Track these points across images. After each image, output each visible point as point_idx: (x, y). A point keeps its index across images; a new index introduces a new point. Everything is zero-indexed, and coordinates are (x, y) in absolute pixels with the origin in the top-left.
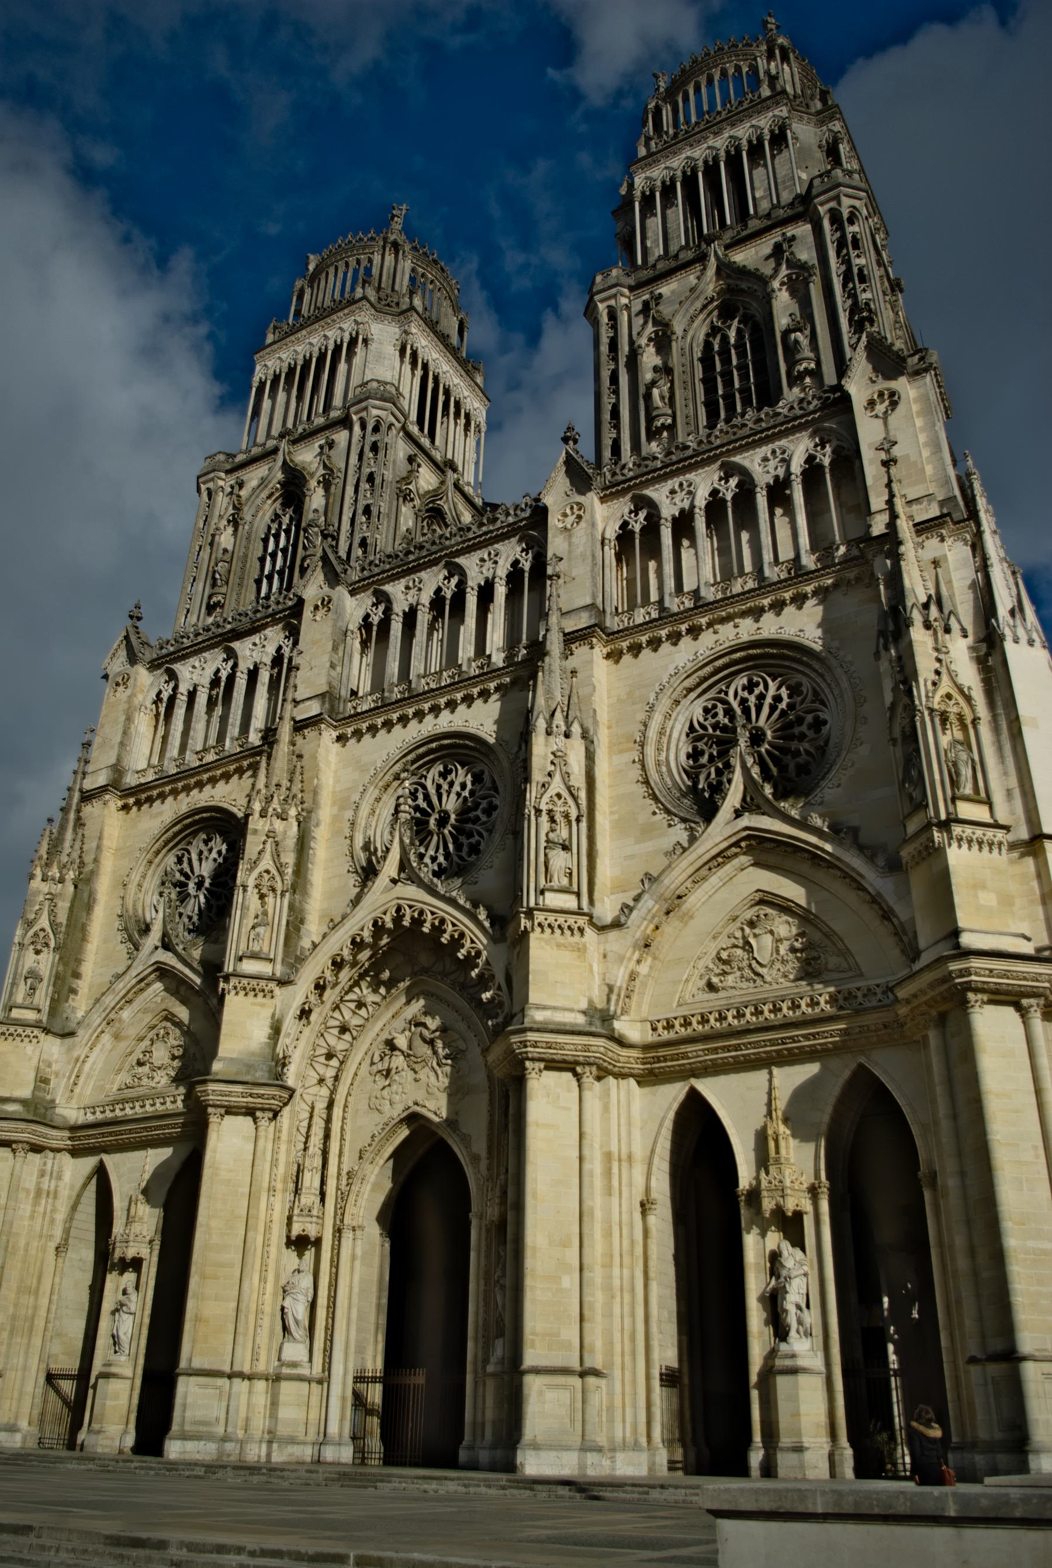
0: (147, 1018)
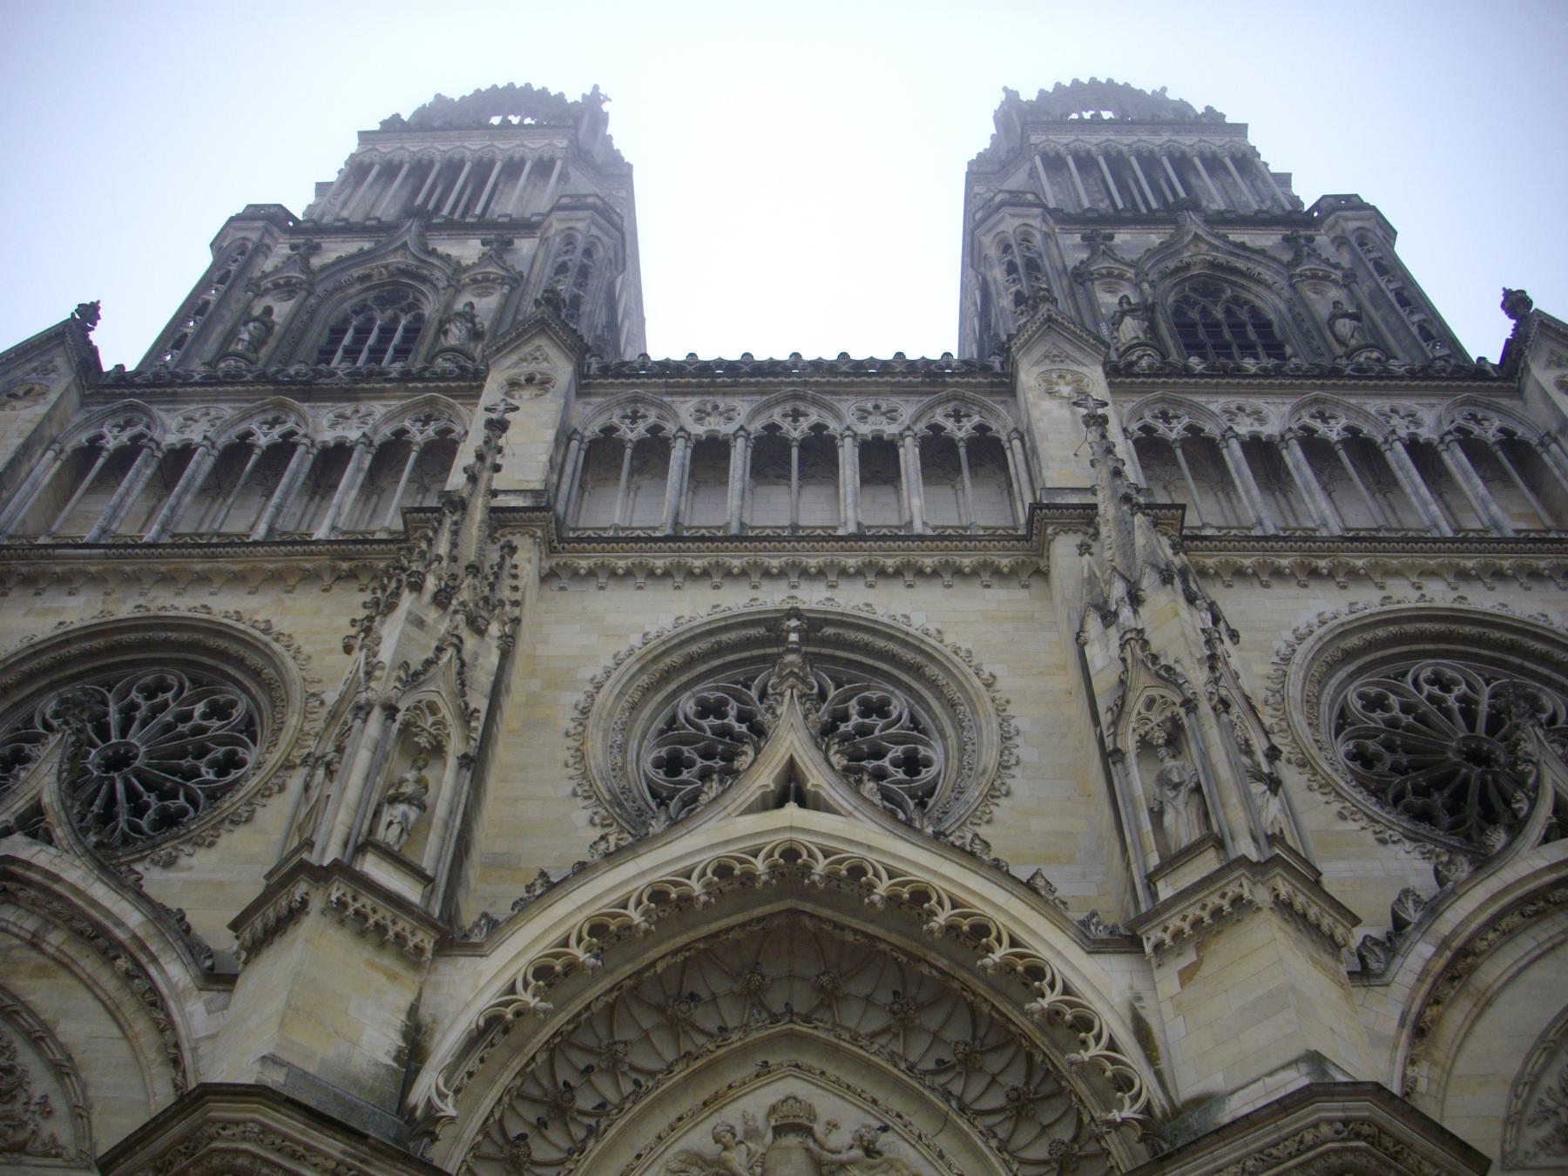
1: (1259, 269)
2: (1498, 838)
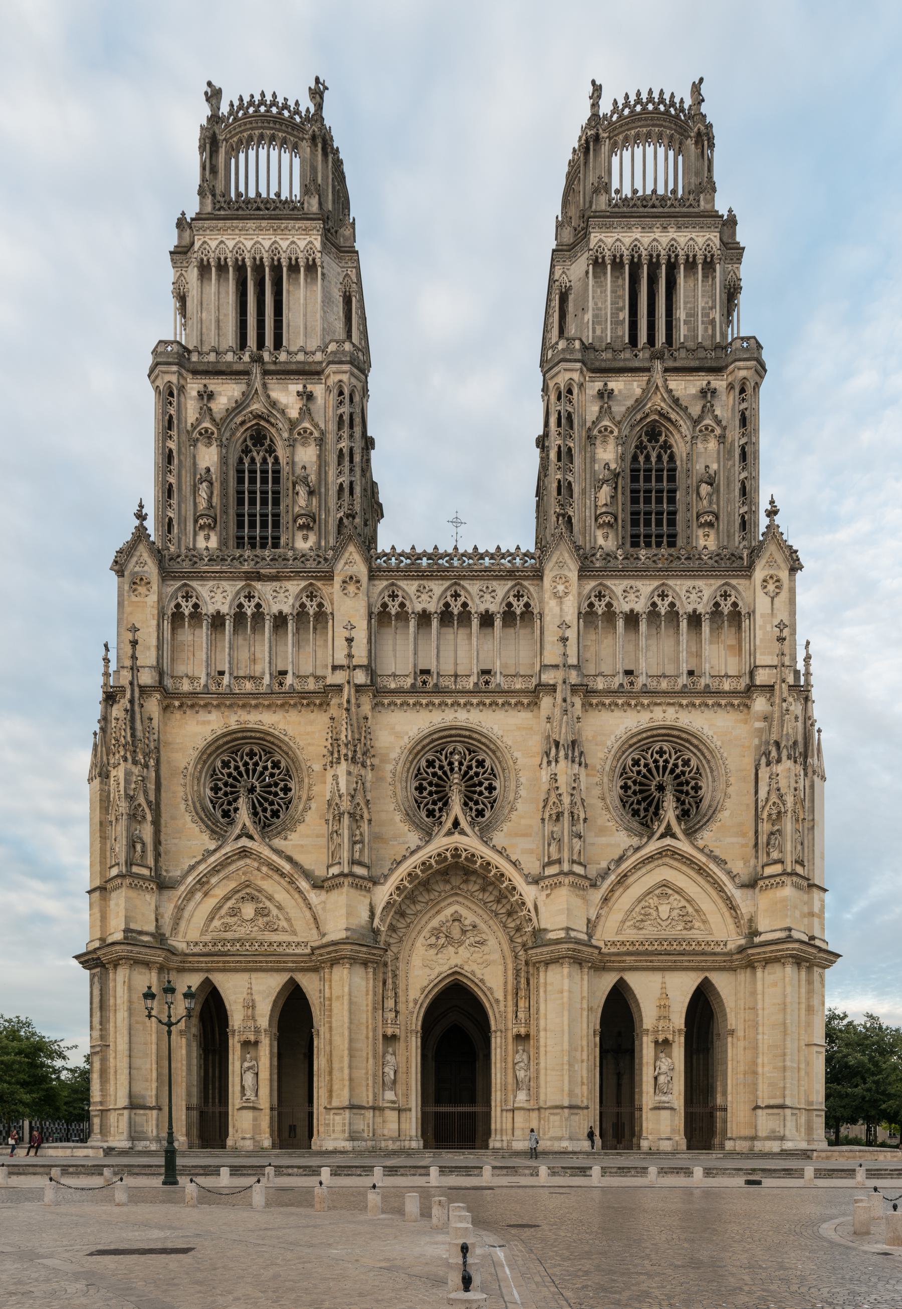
0: (233, 885)
1: (681, 422)
2: (645, 840)
